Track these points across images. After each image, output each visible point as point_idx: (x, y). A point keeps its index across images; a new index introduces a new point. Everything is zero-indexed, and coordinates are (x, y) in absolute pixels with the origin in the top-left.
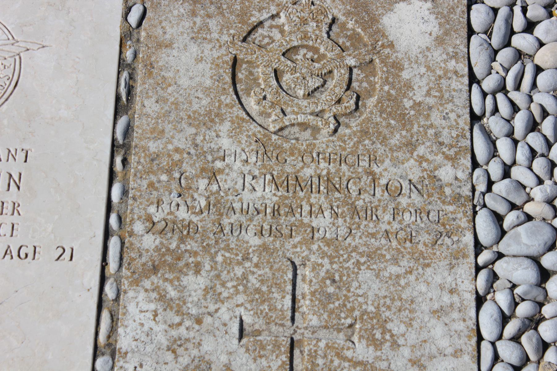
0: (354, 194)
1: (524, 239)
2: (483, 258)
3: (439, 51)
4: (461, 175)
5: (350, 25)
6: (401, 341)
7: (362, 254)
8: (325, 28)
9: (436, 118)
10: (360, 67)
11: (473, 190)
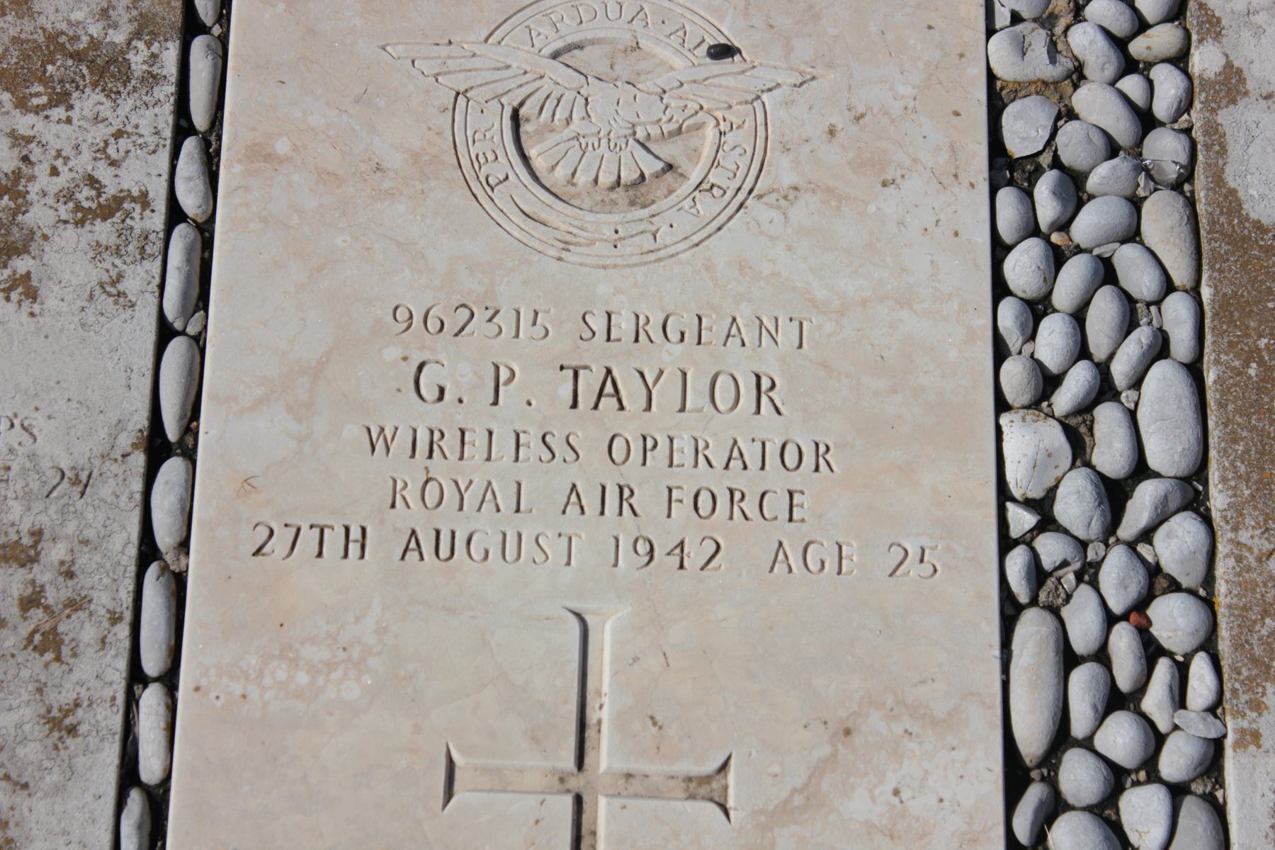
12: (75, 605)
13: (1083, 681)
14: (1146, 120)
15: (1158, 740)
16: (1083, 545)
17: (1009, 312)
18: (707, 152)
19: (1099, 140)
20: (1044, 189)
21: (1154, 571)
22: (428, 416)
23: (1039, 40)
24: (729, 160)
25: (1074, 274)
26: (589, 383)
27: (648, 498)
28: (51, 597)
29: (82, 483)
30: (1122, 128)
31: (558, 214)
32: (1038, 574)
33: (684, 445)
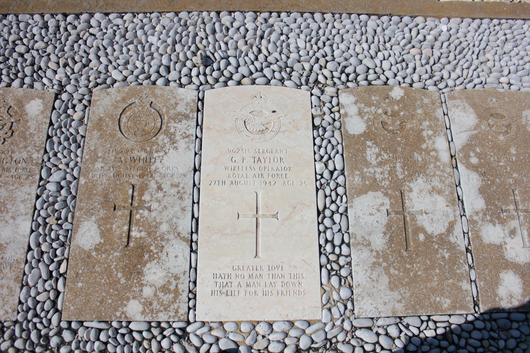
0: (5, 163)
1: (55, 177)
2: (41, 184)
3: (42, 115)
4: (40, 156)
5: (15, 108)
6: (10, 211)
7: (2, 183)
8: (7, 109)
9: (36, 138)
10: (16, 122)
11: (43, 160)
12: (184, 193)
13: (328, 200)
14: (334, 120)
15: (339, 207)
16: (327, 180)
17: (316, 147)
18: (272, 126)
19: (328, 123)
20: (320, 130)
21: (337, 184)
22: (233, 165)
23: (319, 109)
24: (275, 127)
25: (325, 142)
26: (256, 159)
27: (265, 175)
28: (181, 192)
29: (185, 176)
30: (331, 121)
31: (251, 135)
32: (321, 185)
33: (270, 168)
